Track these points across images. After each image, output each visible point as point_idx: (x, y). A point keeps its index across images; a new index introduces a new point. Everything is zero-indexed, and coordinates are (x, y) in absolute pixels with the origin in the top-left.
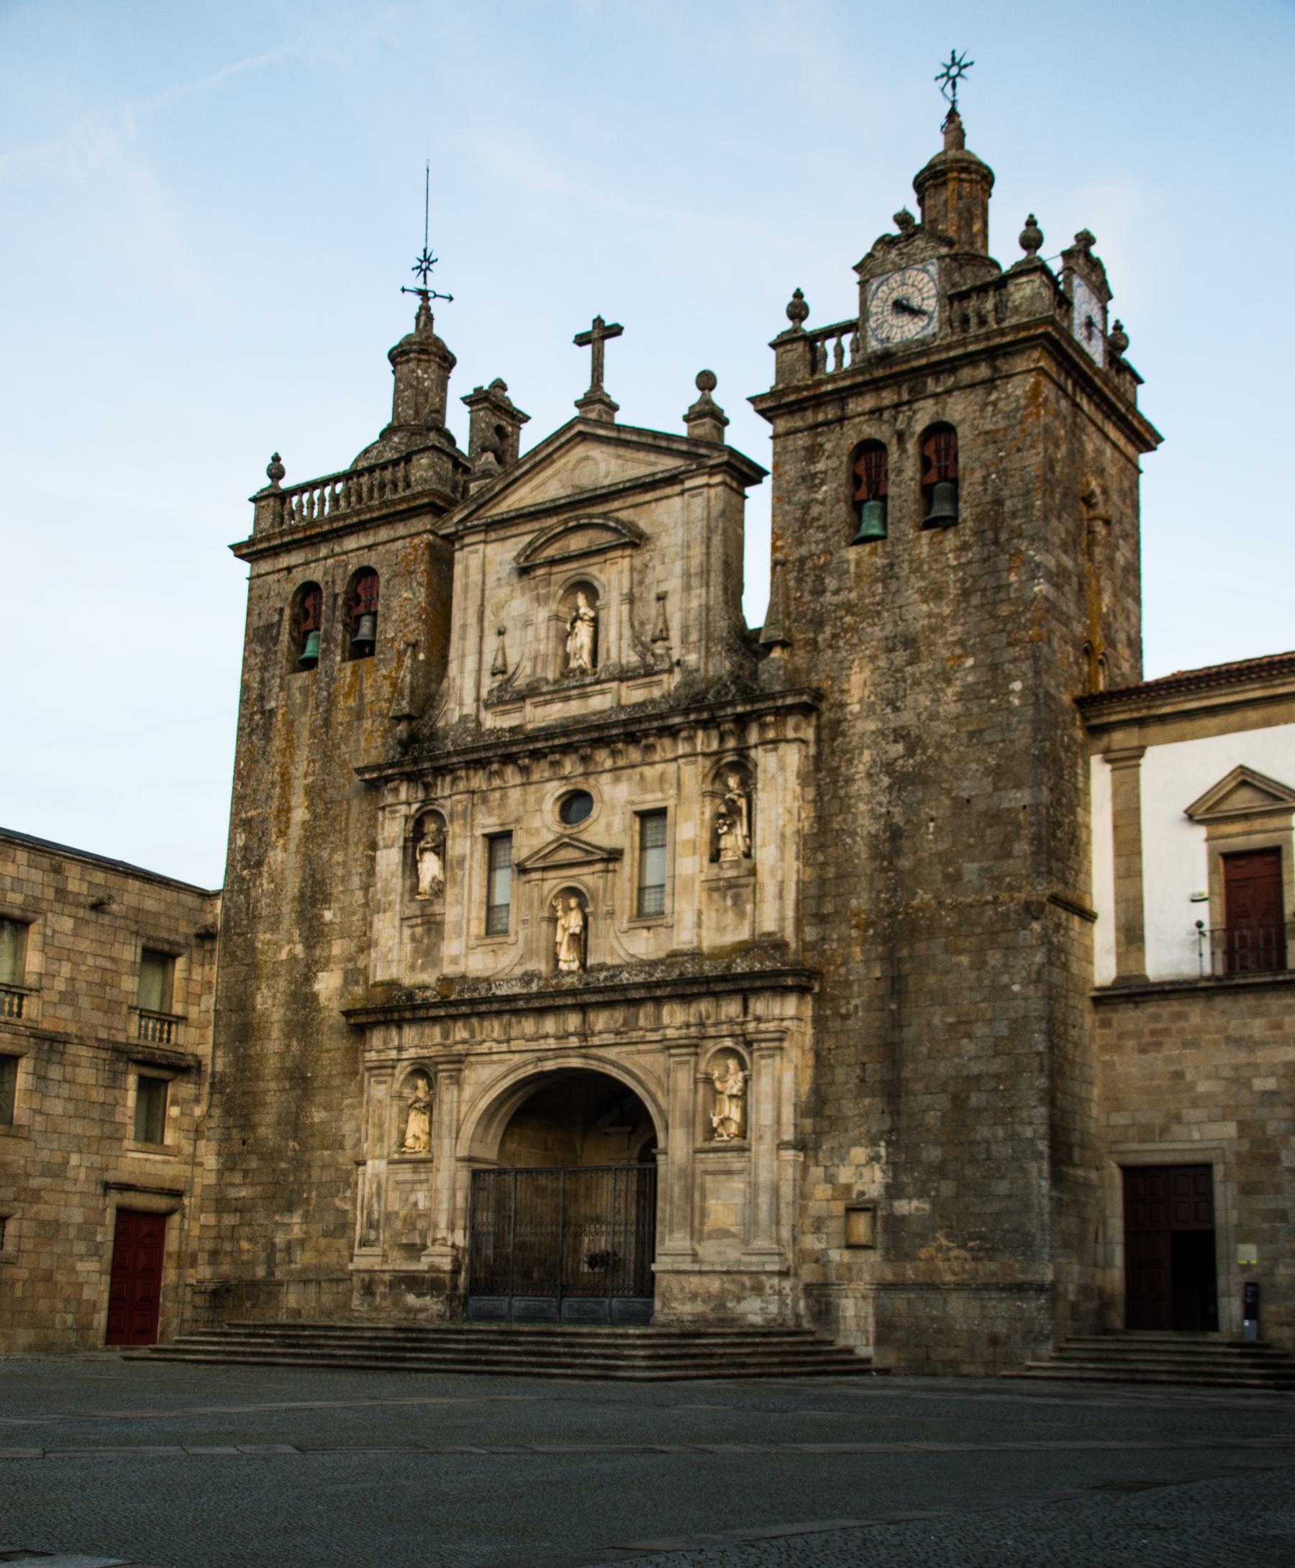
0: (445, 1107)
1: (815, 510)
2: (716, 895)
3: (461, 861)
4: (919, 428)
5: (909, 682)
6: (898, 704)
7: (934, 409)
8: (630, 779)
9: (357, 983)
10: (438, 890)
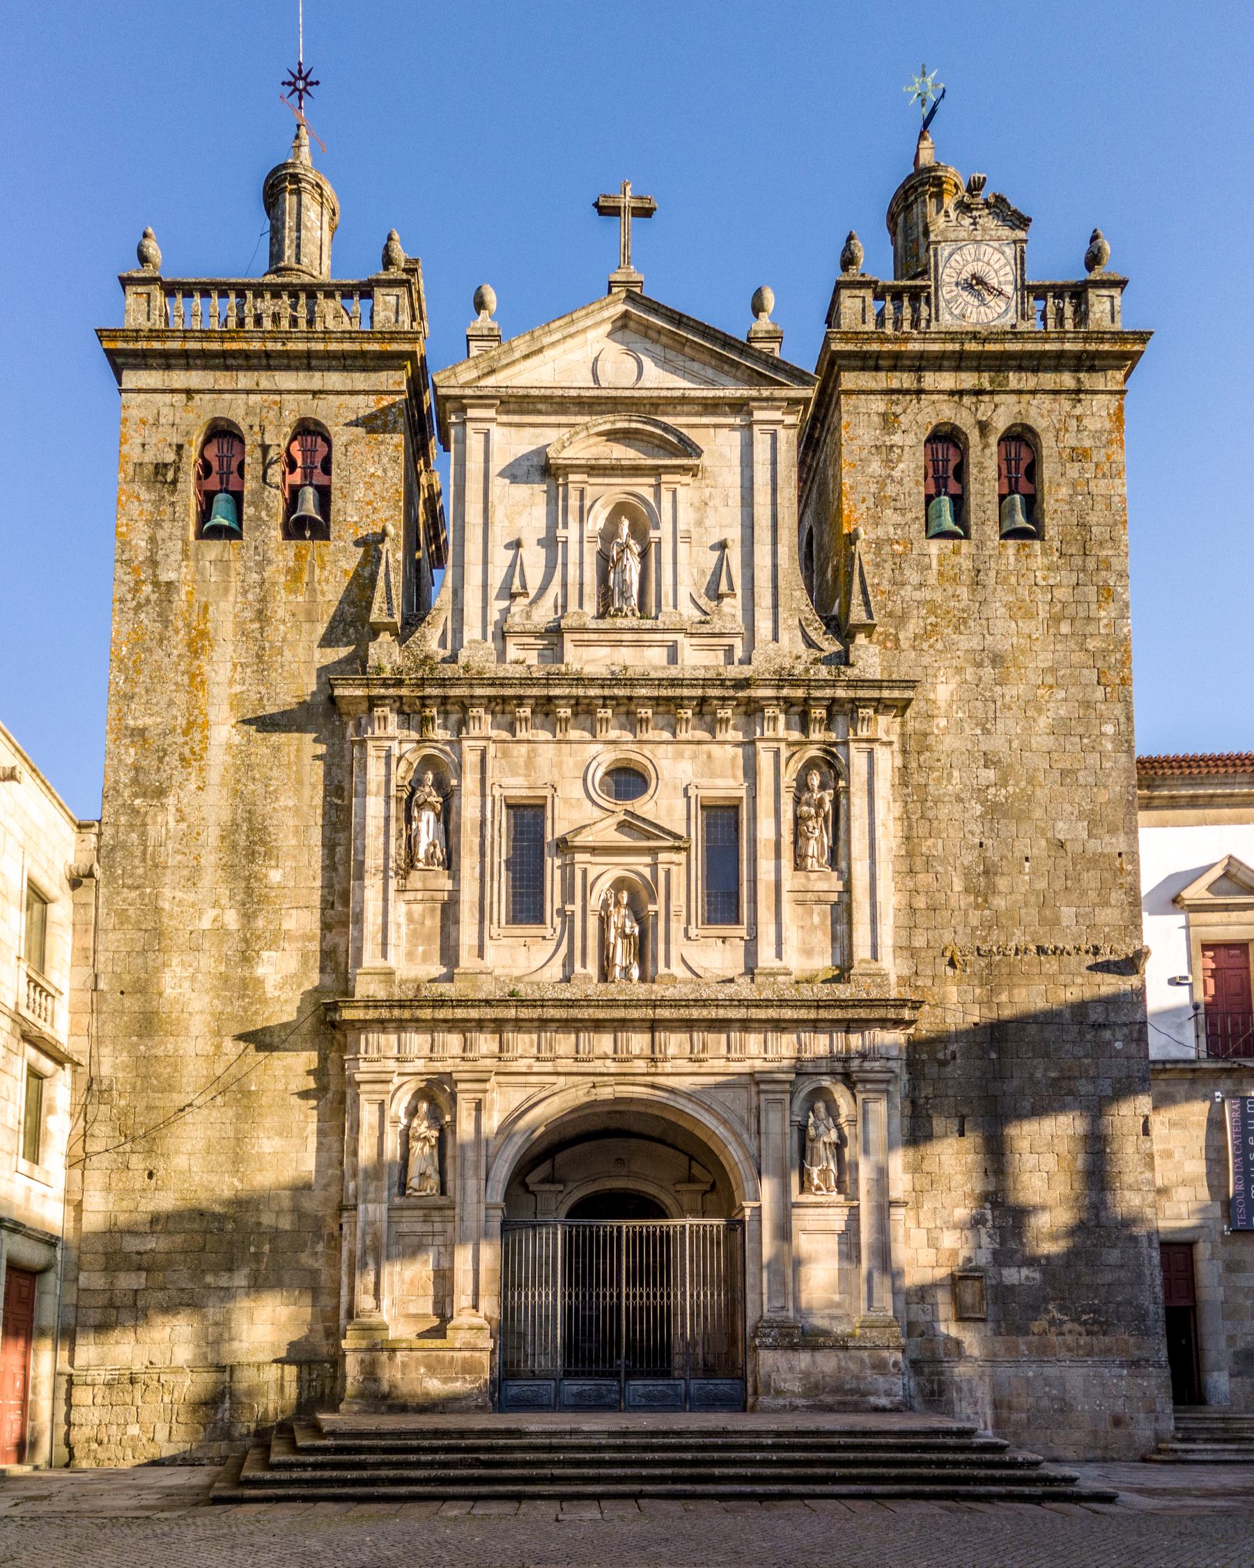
5: (999, 703)
6: (988, 726)
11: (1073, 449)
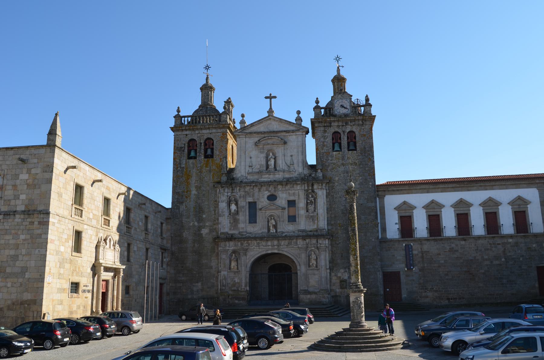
0: (242, 260)
1: (325, 144)
2: (308, 219)
3: (243, 207)
4: (348, 131)
7: (351, 128)
8: (286, 193)
9: (214, 232)
10: (237, 212)
11: (362, 134)
